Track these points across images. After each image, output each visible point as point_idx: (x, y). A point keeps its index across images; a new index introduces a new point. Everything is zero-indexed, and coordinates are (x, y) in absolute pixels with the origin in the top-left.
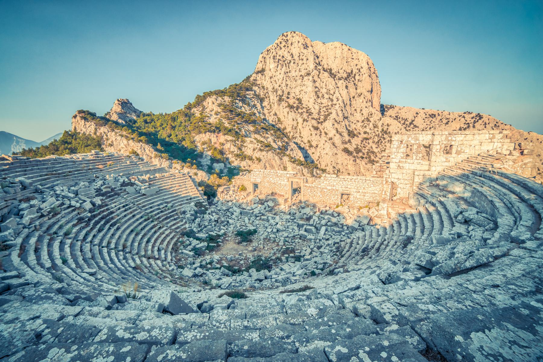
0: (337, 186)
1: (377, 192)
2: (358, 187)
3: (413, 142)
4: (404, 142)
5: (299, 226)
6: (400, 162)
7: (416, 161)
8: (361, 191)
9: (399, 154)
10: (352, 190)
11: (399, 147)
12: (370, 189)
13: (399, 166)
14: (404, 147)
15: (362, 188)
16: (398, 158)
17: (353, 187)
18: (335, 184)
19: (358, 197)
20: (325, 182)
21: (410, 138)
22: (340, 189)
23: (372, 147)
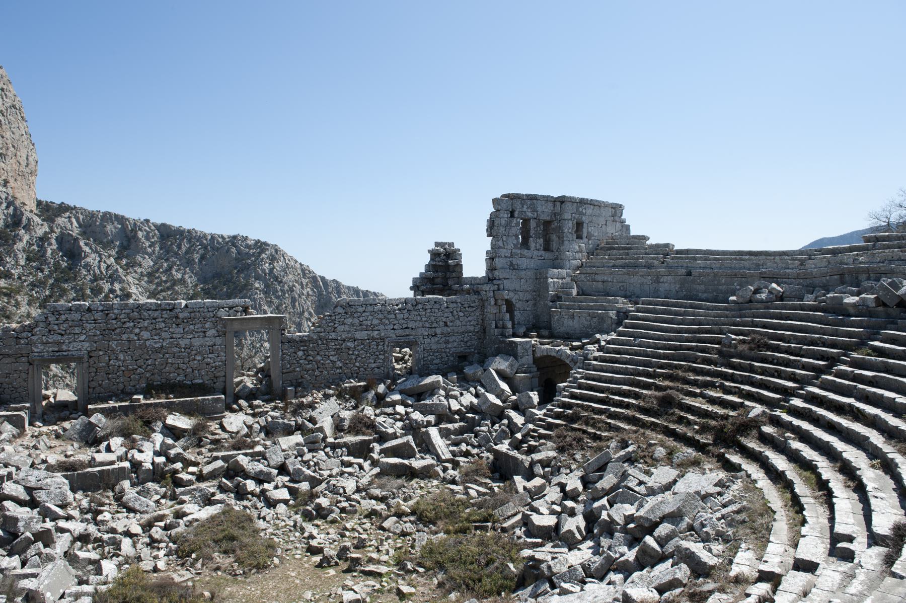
0: (381, 327)
1: (472, 328)
2: (432, 323)
3: (530, 215)
4: (516, 214)
5: (362, 450)
7: (536, 253)
8: (438, 331)
9: (510, 239)
10: (419, 332)
11: (508, 225)
12: (458, 323)
13: (511, 264)
15: (441, 324)
16: (509, 247)
17: (421, 324)
18: (376, 322)
19: (434, 347)
20: (349, 321)
21: (525, 206)
22: (392, 334)
23: (29, 316)
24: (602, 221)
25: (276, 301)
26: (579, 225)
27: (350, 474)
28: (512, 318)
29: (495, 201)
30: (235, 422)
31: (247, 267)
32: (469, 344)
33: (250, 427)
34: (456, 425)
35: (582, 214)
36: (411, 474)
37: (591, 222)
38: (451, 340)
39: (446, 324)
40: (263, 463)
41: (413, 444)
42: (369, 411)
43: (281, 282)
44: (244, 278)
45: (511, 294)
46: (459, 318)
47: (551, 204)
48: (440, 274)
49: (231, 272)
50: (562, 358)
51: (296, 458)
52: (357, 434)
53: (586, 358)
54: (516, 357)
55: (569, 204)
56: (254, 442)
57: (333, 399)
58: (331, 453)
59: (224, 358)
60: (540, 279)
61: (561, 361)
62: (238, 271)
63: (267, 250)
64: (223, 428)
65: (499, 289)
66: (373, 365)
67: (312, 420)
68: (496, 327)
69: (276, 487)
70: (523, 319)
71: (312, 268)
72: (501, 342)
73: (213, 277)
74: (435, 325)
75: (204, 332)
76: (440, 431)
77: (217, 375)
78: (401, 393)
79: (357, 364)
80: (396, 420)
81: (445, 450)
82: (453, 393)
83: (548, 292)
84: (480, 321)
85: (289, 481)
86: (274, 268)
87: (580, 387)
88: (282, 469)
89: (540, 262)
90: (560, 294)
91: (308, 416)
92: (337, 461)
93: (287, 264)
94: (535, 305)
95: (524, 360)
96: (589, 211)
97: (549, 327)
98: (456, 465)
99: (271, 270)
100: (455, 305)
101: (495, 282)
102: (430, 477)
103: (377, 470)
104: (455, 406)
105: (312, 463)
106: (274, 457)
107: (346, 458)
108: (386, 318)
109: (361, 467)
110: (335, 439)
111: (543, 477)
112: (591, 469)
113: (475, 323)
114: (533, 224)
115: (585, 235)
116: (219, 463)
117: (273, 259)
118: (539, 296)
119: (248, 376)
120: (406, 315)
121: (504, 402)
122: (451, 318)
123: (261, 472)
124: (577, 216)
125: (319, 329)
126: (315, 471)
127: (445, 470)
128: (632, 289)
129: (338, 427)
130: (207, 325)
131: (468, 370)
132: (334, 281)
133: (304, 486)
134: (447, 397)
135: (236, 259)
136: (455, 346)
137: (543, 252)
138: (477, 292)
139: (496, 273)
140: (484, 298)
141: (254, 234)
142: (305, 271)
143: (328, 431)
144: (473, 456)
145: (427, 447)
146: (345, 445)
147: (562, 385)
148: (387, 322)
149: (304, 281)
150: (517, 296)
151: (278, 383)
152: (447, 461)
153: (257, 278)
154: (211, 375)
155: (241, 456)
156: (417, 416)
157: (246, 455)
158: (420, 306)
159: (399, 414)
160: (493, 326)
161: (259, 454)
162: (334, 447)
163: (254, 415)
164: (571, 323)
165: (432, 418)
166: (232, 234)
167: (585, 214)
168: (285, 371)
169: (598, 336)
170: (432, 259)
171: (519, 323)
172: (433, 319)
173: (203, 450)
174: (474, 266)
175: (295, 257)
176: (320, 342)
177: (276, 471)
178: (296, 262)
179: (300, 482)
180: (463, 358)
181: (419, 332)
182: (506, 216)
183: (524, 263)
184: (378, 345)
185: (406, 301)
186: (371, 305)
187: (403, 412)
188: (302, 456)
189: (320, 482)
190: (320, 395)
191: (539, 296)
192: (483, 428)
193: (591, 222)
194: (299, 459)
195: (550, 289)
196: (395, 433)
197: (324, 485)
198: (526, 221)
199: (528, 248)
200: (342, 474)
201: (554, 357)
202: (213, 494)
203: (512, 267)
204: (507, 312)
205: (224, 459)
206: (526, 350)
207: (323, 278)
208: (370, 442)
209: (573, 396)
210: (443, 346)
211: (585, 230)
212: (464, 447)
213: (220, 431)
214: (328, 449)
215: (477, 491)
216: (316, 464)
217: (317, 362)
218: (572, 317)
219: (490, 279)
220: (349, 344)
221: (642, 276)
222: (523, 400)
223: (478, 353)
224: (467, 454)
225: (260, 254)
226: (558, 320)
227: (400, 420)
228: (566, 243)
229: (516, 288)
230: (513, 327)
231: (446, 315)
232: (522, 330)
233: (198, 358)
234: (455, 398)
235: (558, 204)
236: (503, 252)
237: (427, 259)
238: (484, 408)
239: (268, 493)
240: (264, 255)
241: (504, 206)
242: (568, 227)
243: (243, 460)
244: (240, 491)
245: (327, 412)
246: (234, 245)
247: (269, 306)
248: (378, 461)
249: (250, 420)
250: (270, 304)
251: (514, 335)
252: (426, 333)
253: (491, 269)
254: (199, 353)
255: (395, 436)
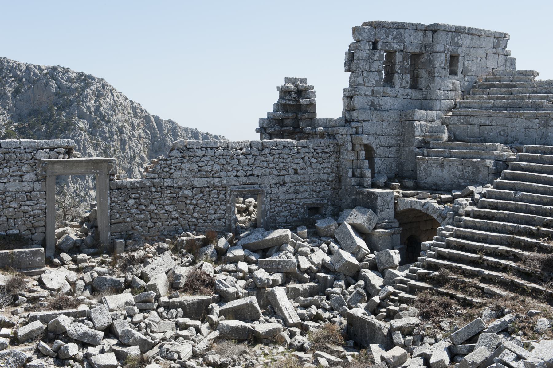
0: (223, 174)
1: (325, 177)
3: (395, 46)
4: (379, 46)
5: (200, 311)
6: (373, 94)
7: (401, 91)
8: (287, 179)
10: (266, 180)
11: (370, 58)
12: (310, 170)
14: (381, 57)
15: (291, 171)
18: (217, 168)
19: (282, 197)
20: (186, 166)
21: (390, 37)
22: (234, 181)
24: (481, 53)
25: (103, 144)
26: (454, 59)
27: (186, 338)
28: (371, 166)
29: (355, 30)
30: (57, 277)
31: (70, 104)
32: (321, 194)
33: (73, 284)
34: (306, 286)
35: (457, 45)
36: (254, 338)
37: (468, 55)
38: (301, 190)
39: (296, 172)
40: (87, 324)
41: (257, 305)
42: (208, 268)
43: (109, 122)
44: (65, 117)
45: (372, 139)
46: (310, 165)
47: (421, 34)
48: (290, 115)
49: (50, 109)
50: (429, 212)
51: (125, 318)
52: (194, 292)
53: (456, 213)
54: (375, 210)
55: (442, 33)
56: (78, 300)
57: (168, 254)
58: (164, 314)
59: (44, 206)
60: (405, 122)
61: (426, 215)
62: (59, 108)
63: (92, 84)
64: (42, 284)
65: (357, 133)
66: (213, 217)
67: (144, 277)
68: (354, 176)
69: (102, 352)
70: (384, 167)
71: (144, 107)
72: (358, 193)
73: (30, 114)
74: (283, 172)
75: (21, 176)
76: (288, 291)
77: (36, 224)
78: (244, 248)
79: (196, 215)
80: (238, 278)
81: (293, 313)
82: (302, 249)
83: (414, 136)
84: (335, 169)
85: (117, 344)
86: (100, 105)
87: (449, 246)
88: (110, 331)
89: (406, 101)
90: (428, 139)
91: (139, 272)
92: (172, 323)
93: (115, 102)
94: (398, 151)
95: (384, 214)
96: (466, 41)
97: (414, 177)
98: (305, 330)
99: (97, 108)
100: (307, 150)
101: (353, 124)
102: (275, 343)
103: (216, 333)
104: (305, 263)
105: (143, 325)
106: (100, 317)
107: (181, 320)
108: (228, 163)
109: (198, 330)
110: (170, 298)
111: (404, 346)
112: (459, 340)
113: (329, 170)
114: (399, 57)
115: (460, 70)
116: (37, 325)
117: (99, 95)
118: (403, 141)
119: (72, 226)
120: (252, 161)
121: (360, 260)
122: (302, 165)
123: (85, 334)
124: (451, 48)
125: (152, 175)
126: (146, 334)
127: (292, 335)
128: (514, 133)
129: (173, 285)
130: (24, 168)
131: (321, 224)
132: (170, 121)
133: (134, 351)
134: (296, 253)
135: (56, 94)
136: (306, 196)
137: (410, 91)
138: (332, 136)
139: (355, 114)
140: (341, 142)
141: (77, 66)
142: (136, 110)
143: (162, 288)
144: (324, 320)
145: (272, 309)
146: (181, 305)
147: (427, 243)
148: (229, 168)
149: (136, 121)
150: (377, 141)
151: (105, 235)
152: (295, 325)
153: (81, 116)
154: (29, 225)
155: (62, 316)
156: (261, 274)
157: (68, 314)
158: (267, 151)
159: (241, 271)
160: (350, 174)
161: (83, 314)
162: (168, 307)
163: (78, 270)
164: (439, 172)
165: (278, 277)
166: (51, 64)
167: (461, 46)
168: (113, 221)
169: (471, 188)
170: (281, 98)
171: (379, 172)
172: (281, 165)
173: (19, 309)
174: (329, 106)
175: (125, 94)
176: (153, 189)
177: (103, 333)
178: (126, 99)
179: (129, 346)
180: (315, 210)
181: (266, 180)
182: (367, 48)
183: (386, 102)
184: (219, 194)
185: (251, 145)
186: (211, 148)
187: (246, 270)
188: (131, 317)
189: (152, 346)
190: (153, 249)
191: (403, 141)
192: (335, 290)
193: (468, 55)
194: (129, 319)
195: (417, 133)
196: (237, 293)
197: (156, 350)
198: (391, 54)
199: (392, 86)
200: (177, 337)
201: (419, 211)
202: (29, 360)
203: (374, 107)
204: (366, 159)
205: (43, 319)
206: (387, 202)
207: (157, 119)
208: (208, 302)
209: (440, 256)
210: (293, 196)
211: (460, 65)
212: (314, 310)
213: (38, 288)
214: (161, 310)
215: (328, 360)
216: (148, 326)
217: (151, 212)
218: (442, 166)
219: (347, 121)
220: (186, 192)
221: (527, 119)
222: (382, 259)
223: (333, 205)
224: (317, 318)
225: (84, 89)
226: (425, 169)
227: (242, 278)
228: (437, 79)
229: (377, 132)
230: (373, 176)
231: (296, 161)
232: (383, 180)
233: (14, 205)
234: (305, 255)
235: (430, 34)
236: (363, 90)
237: (275, 97)
238: (337, 266)
239: (92, 358)
240: (89, 91)
241: (365, 36)
242: (441, 61)
243: (65, 321)
244: (61, 356)
245: (161, 267)
246: (53, 77)
247: (95, 150)
248: (217, 324)
249: (73, 276)
250: (96, 146)
251: (374, 186)
252: (274, 182)
253: (349, 109)
254: (15, 200)
255: (236, 296)
